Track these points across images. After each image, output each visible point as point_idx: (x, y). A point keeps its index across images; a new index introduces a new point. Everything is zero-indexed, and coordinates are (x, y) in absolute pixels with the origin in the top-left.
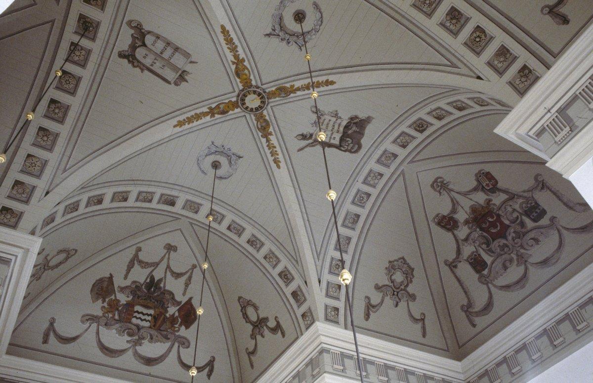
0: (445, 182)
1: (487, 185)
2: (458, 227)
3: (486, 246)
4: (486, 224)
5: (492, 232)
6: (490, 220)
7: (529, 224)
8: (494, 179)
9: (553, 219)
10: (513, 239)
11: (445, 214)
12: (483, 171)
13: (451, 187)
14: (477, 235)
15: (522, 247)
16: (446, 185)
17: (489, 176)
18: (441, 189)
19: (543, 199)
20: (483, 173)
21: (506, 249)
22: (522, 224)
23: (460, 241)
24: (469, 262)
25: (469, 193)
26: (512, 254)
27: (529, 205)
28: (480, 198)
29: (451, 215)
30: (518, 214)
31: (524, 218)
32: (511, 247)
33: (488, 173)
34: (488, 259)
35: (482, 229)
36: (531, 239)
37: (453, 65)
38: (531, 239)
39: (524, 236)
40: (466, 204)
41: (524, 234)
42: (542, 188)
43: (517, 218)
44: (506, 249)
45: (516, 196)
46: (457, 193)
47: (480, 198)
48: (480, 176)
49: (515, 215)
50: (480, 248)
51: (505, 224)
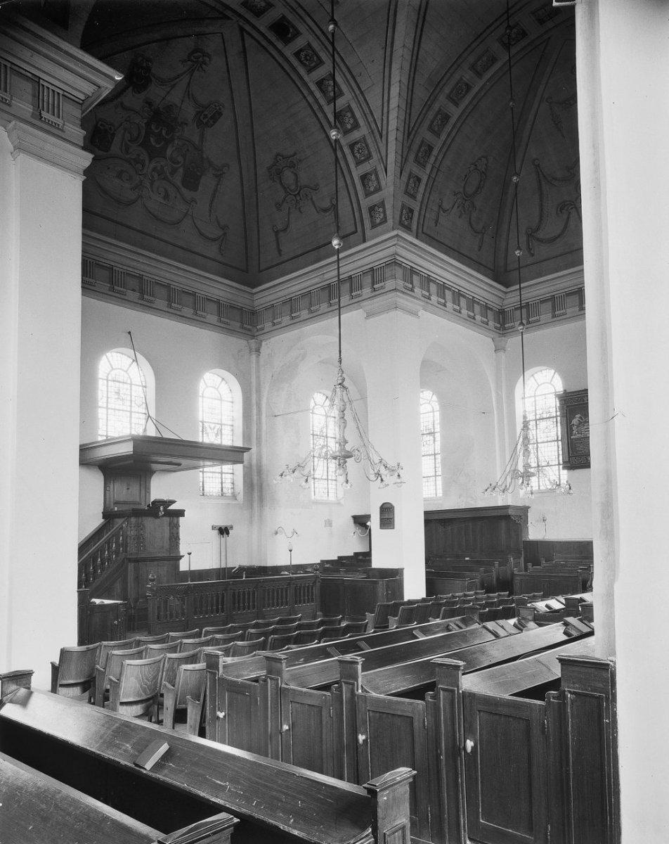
0: (204, 66)
1: (206, 116)
2: (139, 93)
3: (129, 139)
4: (157, 129)
5: (150, 141)
6: (164, 132)
7: (178, 179)
8: (214, 123)
9: (193, 200)
10: (155, 168)
11: (153, 71)
12: (222, 109)
13: (196, 74)
14: (137, 121)
15: (152, 184)
16: (200, 68)
17: (217, 116)
18: (192, 61)
19: (207, 181)
20: (220, 109)
21: (139, 166)
22: (174, 171)
23: (119, 100)
24: (97, 125)
25: (190, 96)
26: (138, 176)
27: (195, 170)
28: (189, 111)
29: (153, 79)
30: (182, 162)
31: (181, 170)
32: (145, 171)
33: (220, 114)
34: (115, 148)
35: (148, 124)
36: (165, 189)
37: (409, 134)
38: (166, 191)
39: (164, 179)
40: (176, 97)
41: (165, 179)
42: (216, 176)
43: (178, 163)
44: (139, 166)
45: (200, 152)
46: (189, 84)
47: (189, 111)
48: (215, 106)
49: (180, 159)
50: (123, 131)
51: (166, 151)
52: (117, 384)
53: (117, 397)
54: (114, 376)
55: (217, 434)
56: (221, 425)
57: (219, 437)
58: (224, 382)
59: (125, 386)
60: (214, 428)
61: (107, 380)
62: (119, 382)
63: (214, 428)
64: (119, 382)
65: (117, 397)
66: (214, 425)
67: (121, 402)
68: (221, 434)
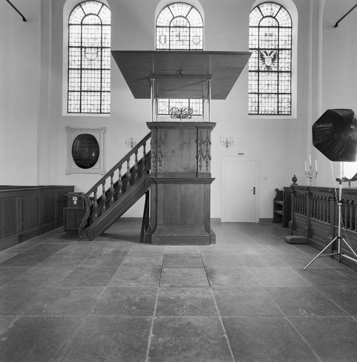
52: (178, 29)
53: (178, 39)
54: (175, 23)
55: (273, 60)
56: (278, 49)
57: (276, 61)
58: (283, 9)
59: (185, 29)
60: (271, 53)
61: (170, 27)
62: (180, 27)
63: (271, 53)
64: (180, 27)
65: (178, 39)
66: (270, 51)
67: (181, 43)
68: (278, 58)
